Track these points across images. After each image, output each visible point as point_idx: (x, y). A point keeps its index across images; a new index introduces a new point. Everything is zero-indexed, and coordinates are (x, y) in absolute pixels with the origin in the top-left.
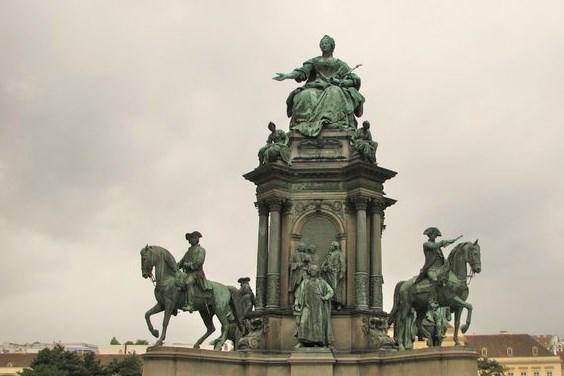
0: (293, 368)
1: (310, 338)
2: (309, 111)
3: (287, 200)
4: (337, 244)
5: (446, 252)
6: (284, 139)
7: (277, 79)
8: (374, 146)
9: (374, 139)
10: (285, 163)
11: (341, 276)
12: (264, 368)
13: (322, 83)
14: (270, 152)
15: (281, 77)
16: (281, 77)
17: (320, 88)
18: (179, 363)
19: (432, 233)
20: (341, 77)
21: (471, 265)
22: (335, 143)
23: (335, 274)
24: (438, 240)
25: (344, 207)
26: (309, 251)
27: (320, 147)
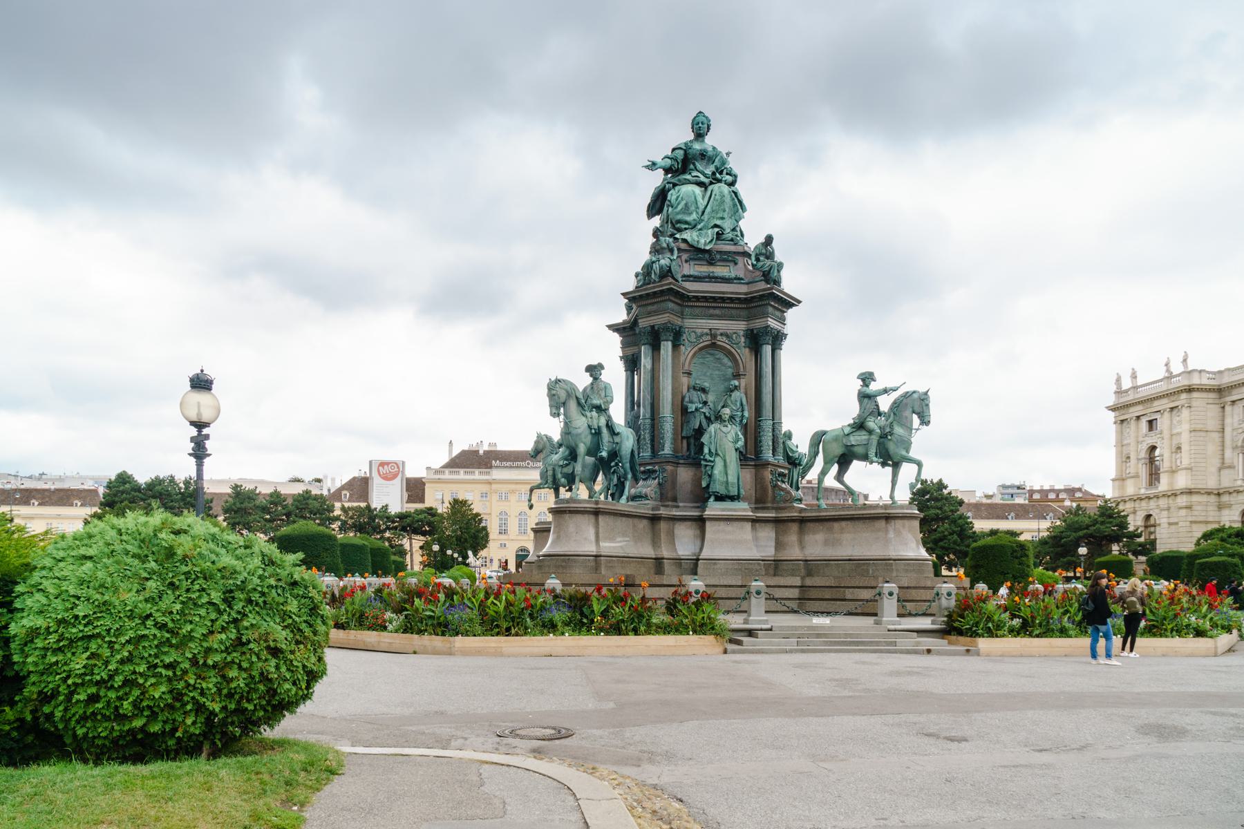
0: (708, 524)
1: (722, 491)
2: (694, 216)
3: (681, 327)
4: (736, 383)
5: (885, 403)
6: (671, 251)
7: (647, 167)
8: (780, 265)
9: (778, 257)
10: (677, 281)
11: (745, 421)
12: (671, 523)
13: (702, 179)
14: (661, 268)
15: (653, 166)
16: (653, 166)
17: (700, 184)
18: (601, 518)
19: (867, 378)
20: (721, 173)
21: (919, 417)
22: (729, 258)
23: (738, 420)
24: (874, 387)
25: (743, 339)
26: (703, 390)
27: (711, 263)
